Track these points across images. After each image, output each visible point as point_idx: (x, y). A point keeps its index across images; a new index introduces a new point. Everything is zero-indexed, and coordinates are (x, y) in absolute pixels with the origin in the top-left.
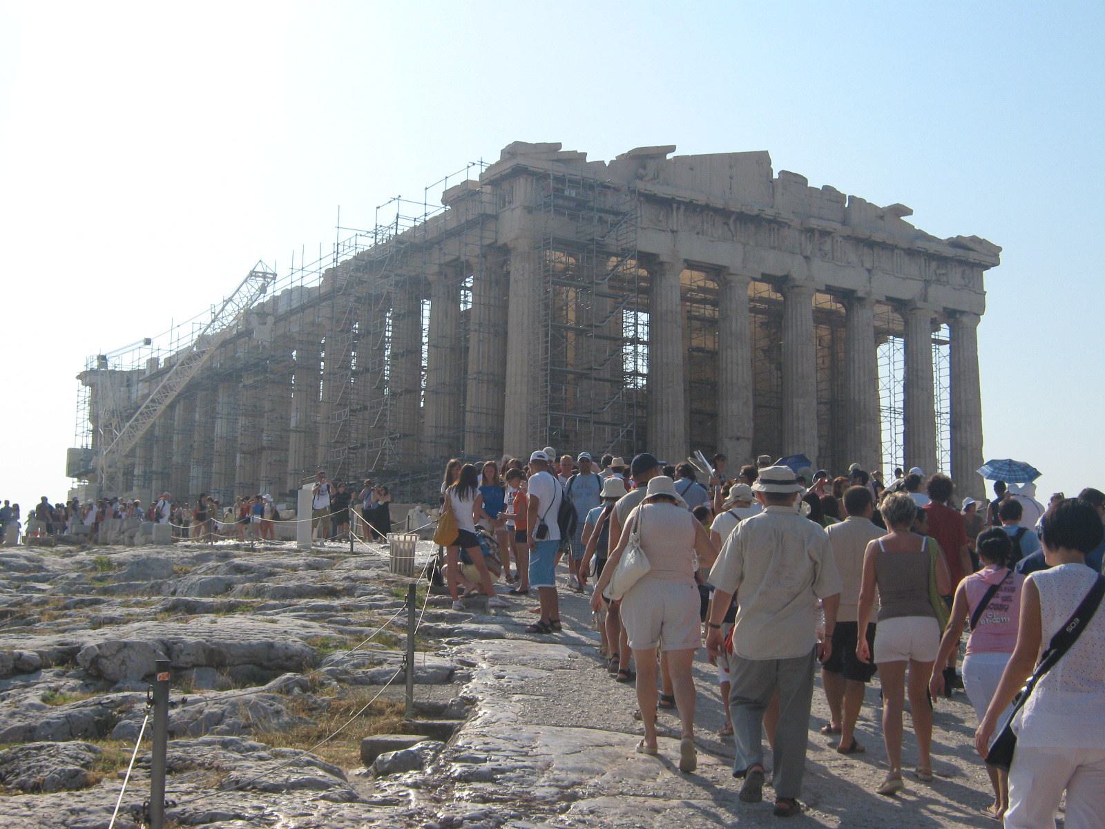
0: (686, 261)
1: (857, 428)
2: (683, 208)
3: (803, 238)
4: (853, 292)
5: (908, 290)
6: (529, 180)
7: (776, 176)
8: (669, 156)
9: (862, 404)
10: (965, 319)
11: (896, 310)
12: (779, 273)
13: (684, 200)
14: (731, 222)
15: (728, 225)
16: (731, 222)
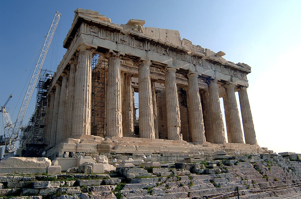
0: (151, 61)
2: (149, 44)
4: (210, 77)
5: (227, 78)
6: (86, 25)
13: (149, 39)
14: (167, 50)
15: (166, 51)
16: (167, 50)
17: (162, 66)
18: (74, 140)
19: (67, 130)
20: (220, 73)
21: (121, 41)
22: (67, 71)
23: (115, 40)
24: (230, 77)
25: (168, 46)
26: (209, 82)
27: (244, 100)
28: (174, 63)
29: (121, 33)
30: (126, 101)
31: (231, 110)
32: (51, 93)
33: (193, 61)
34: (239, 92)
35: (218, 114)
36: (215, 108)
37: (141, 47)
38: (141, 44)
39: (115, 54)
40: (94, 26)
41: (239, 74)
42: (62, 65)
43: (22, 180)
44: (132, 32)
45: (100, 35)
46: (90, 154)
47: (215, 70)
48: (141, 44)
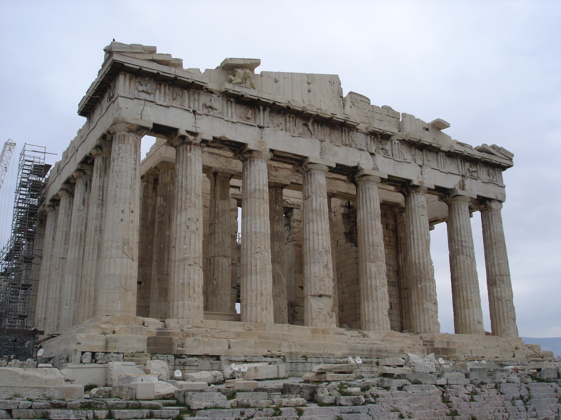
0: (272, 151)
1: (419, 286)
3: (369, 137)
4: (409, 181)
5: (450, 182)
7: (344, 95)
8: (257, 71)
9: (422, 267)
10: (494, 205)
11: (441, 199)
12: (351, 163)
14: (310, 124)
16: (310, 124)
17: (295, 160)
18: (102, 328)
19: (87, 302)
20: (434, 171)
21: (206, 111)
22: (86, 167)
23: (192, 106)
24: (460, 178)
25: (311, 115)
26: (406, 190)
27: (492, 233)
28: (322, 153)
29: (205, 90)
30: (217, 235)
31: (458, 257)
32: (47, 209)
33: (369, 143)
34: (482, 211)
35: (424, 267)
36: (418, 252)
37: (249, 120)
38: (250, 114)
39: (191, 138)
40: (147, 78)
41: (483, 173)
42: (74, 151)
43: (31, 408)
44: (229, 87)
45: (159, 97)
46: (133, 356)
47: (421, 164)
48: (250, 114)
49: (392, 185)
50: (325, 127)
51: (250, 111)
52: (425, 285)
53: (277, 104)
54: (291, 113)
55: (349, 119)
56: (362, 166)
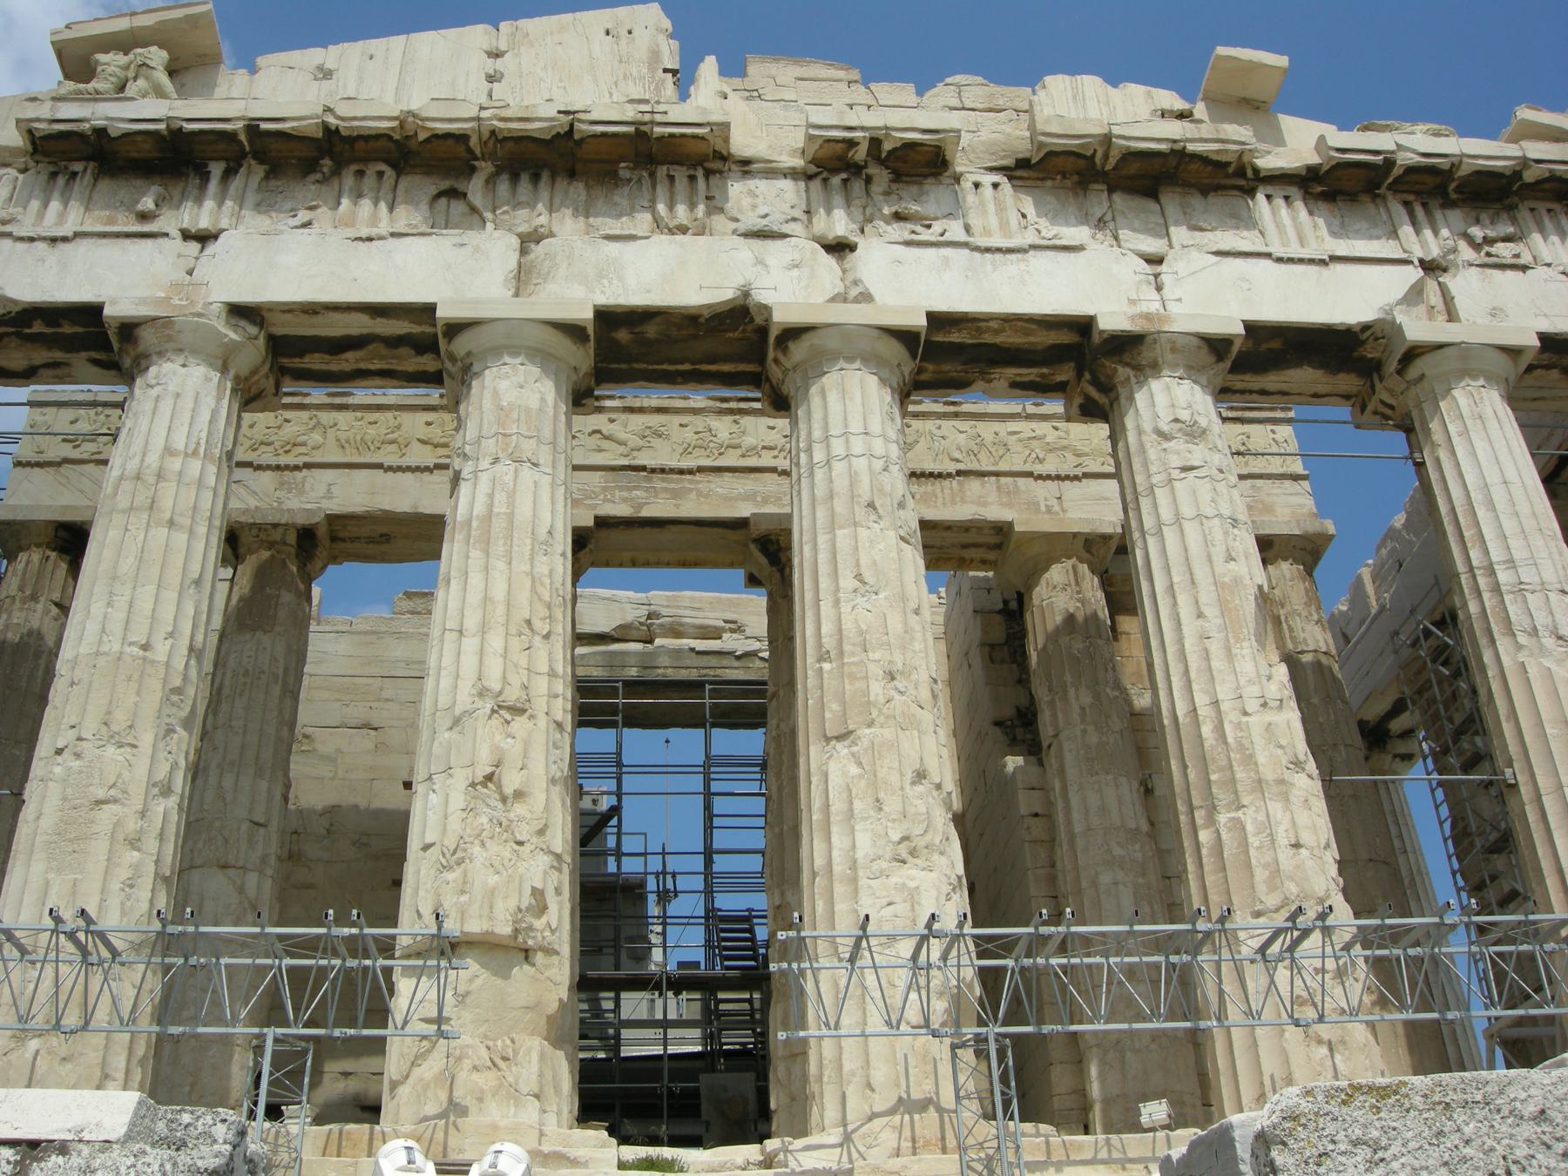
0: (239, 312)
4: (1084, 325)
25: (462, 138)
26: (1095, 382)
28: (522, 279)
36: (1182, 653)
49: (1042, 388)
50: (561, 183)
51: (155, 189)
52: (1238, 826)
53: (264, 126)
54: (367, 159)
55: (658, 118)
56: (762, 296)
